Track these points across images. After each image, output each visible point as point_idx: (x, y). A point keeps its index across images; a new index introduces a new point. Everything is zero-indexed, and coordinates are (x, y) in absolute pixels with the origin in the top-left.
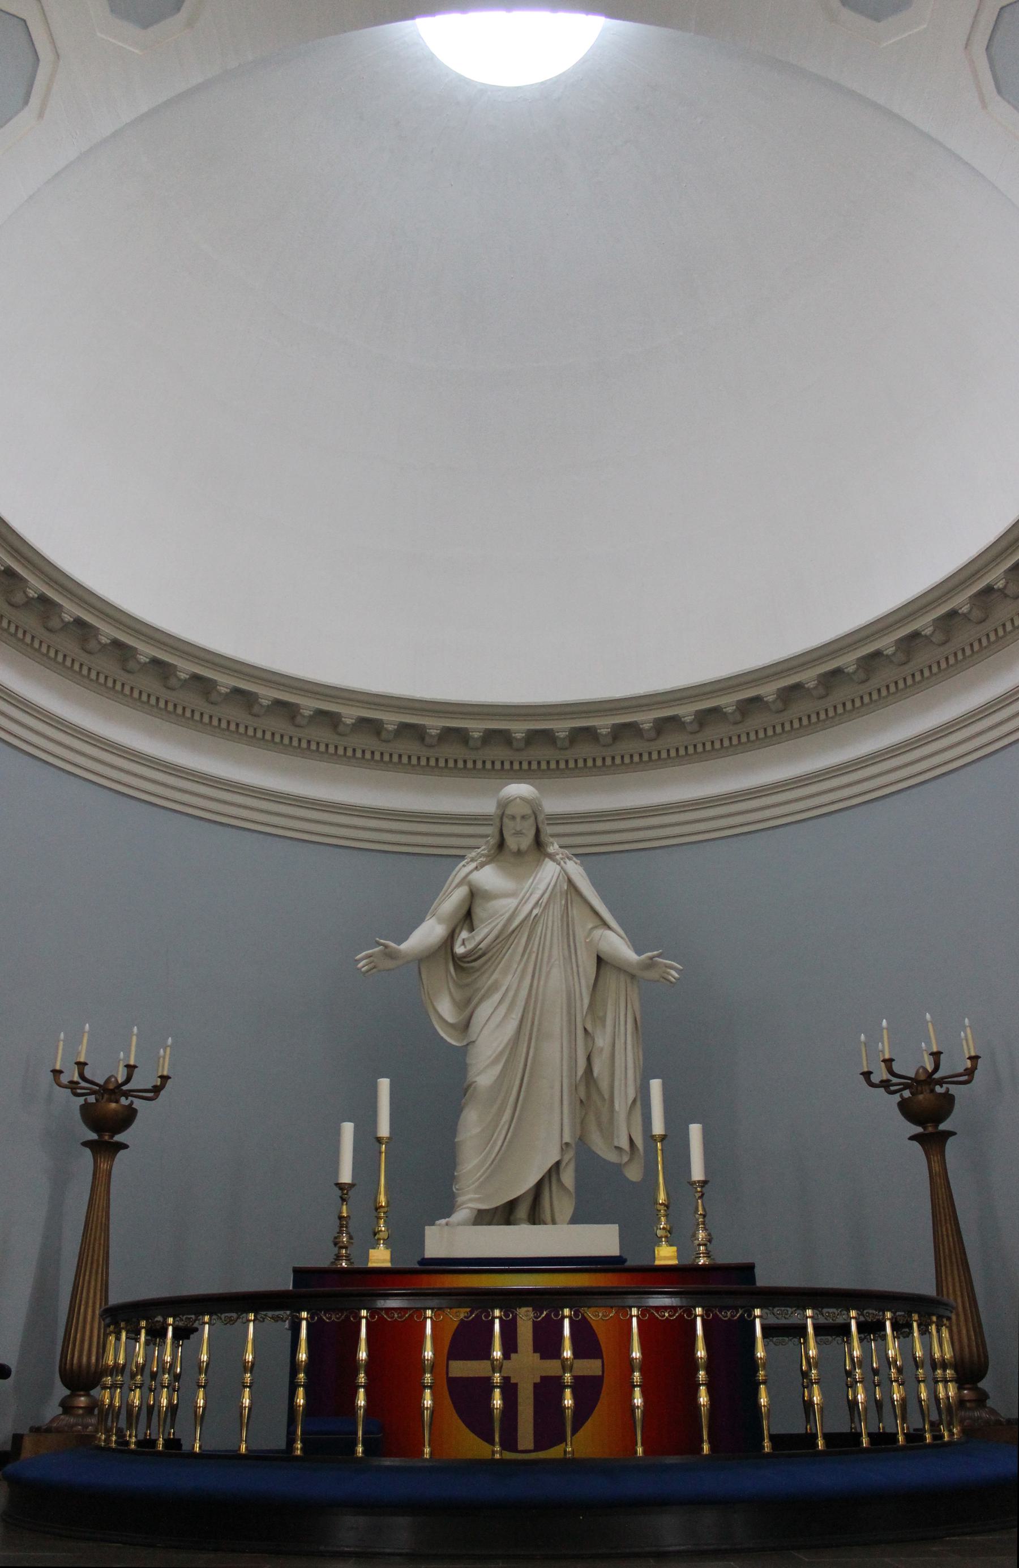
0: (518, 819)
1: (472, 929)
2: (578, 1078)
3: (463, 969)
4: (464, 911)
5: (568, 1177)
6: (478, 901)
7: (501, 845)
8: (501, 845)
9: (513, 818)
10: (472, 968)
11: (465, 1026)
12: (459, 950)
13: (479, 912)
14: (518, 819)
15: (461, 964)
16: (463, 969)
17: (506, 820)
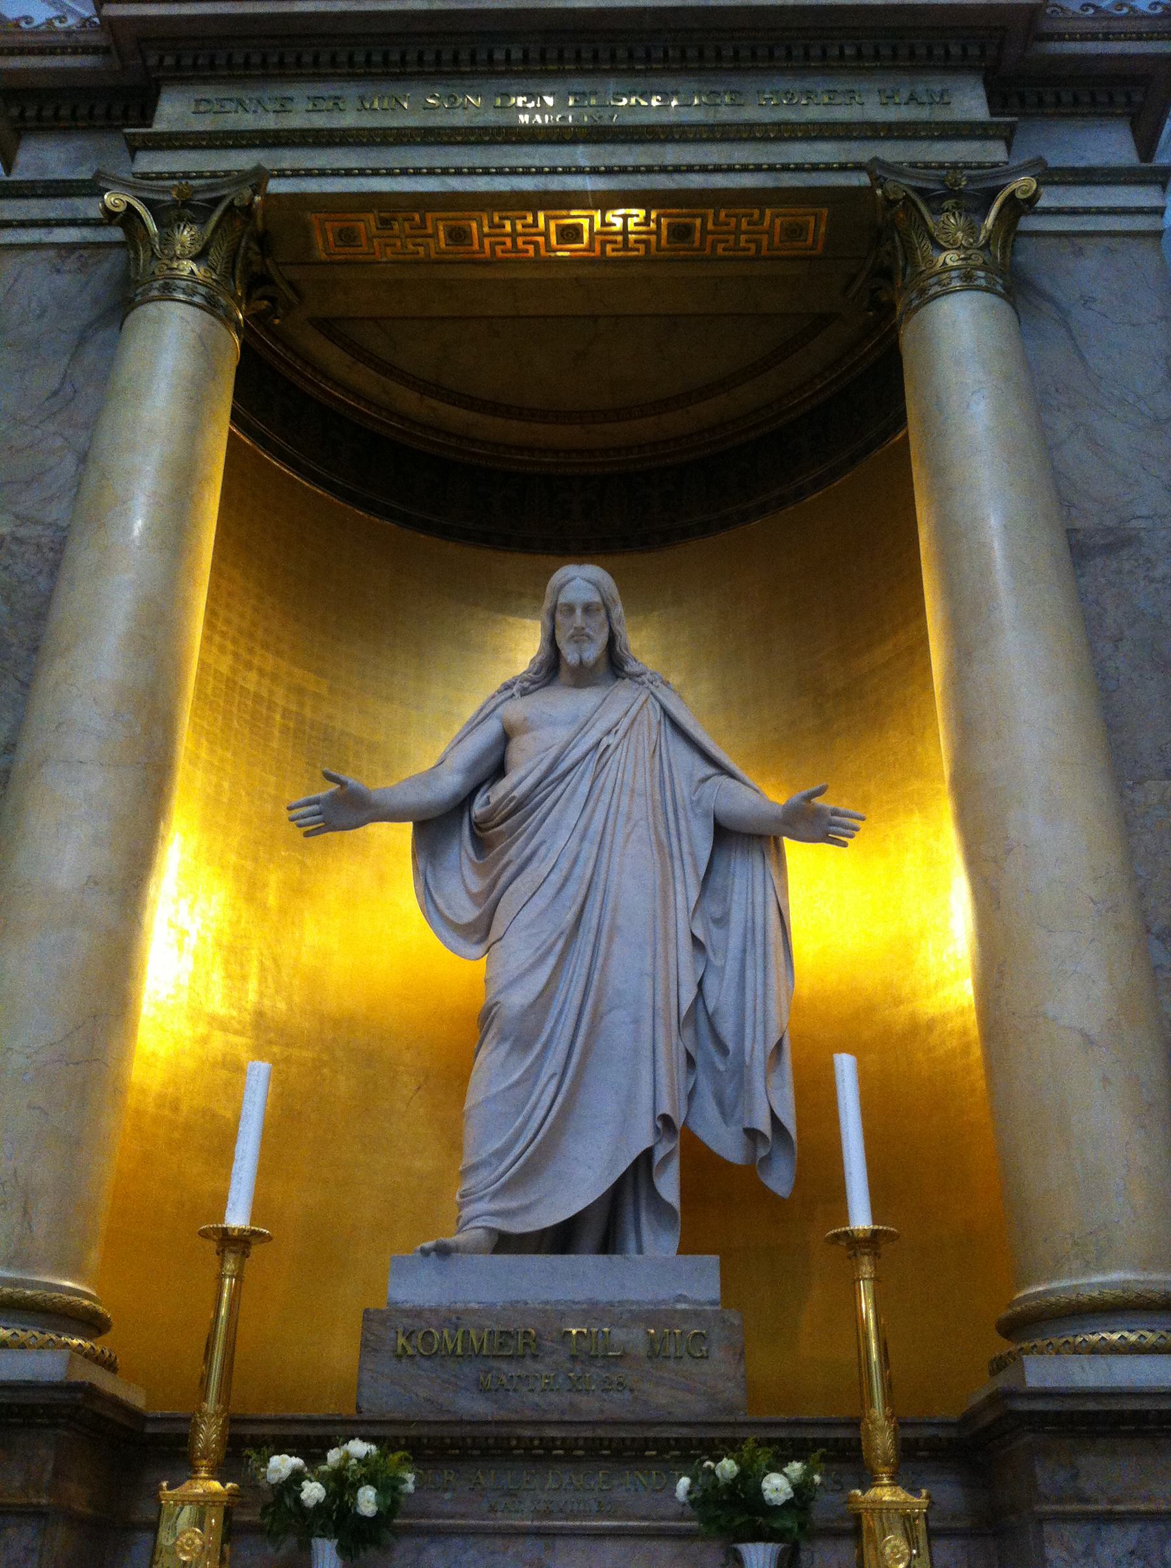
0: (579, 612)
2: (685, 1007)
4: (493, 759)
5: (669, 1186)
9: (570, 609)
10: (501, 833)
14: (579, 612)
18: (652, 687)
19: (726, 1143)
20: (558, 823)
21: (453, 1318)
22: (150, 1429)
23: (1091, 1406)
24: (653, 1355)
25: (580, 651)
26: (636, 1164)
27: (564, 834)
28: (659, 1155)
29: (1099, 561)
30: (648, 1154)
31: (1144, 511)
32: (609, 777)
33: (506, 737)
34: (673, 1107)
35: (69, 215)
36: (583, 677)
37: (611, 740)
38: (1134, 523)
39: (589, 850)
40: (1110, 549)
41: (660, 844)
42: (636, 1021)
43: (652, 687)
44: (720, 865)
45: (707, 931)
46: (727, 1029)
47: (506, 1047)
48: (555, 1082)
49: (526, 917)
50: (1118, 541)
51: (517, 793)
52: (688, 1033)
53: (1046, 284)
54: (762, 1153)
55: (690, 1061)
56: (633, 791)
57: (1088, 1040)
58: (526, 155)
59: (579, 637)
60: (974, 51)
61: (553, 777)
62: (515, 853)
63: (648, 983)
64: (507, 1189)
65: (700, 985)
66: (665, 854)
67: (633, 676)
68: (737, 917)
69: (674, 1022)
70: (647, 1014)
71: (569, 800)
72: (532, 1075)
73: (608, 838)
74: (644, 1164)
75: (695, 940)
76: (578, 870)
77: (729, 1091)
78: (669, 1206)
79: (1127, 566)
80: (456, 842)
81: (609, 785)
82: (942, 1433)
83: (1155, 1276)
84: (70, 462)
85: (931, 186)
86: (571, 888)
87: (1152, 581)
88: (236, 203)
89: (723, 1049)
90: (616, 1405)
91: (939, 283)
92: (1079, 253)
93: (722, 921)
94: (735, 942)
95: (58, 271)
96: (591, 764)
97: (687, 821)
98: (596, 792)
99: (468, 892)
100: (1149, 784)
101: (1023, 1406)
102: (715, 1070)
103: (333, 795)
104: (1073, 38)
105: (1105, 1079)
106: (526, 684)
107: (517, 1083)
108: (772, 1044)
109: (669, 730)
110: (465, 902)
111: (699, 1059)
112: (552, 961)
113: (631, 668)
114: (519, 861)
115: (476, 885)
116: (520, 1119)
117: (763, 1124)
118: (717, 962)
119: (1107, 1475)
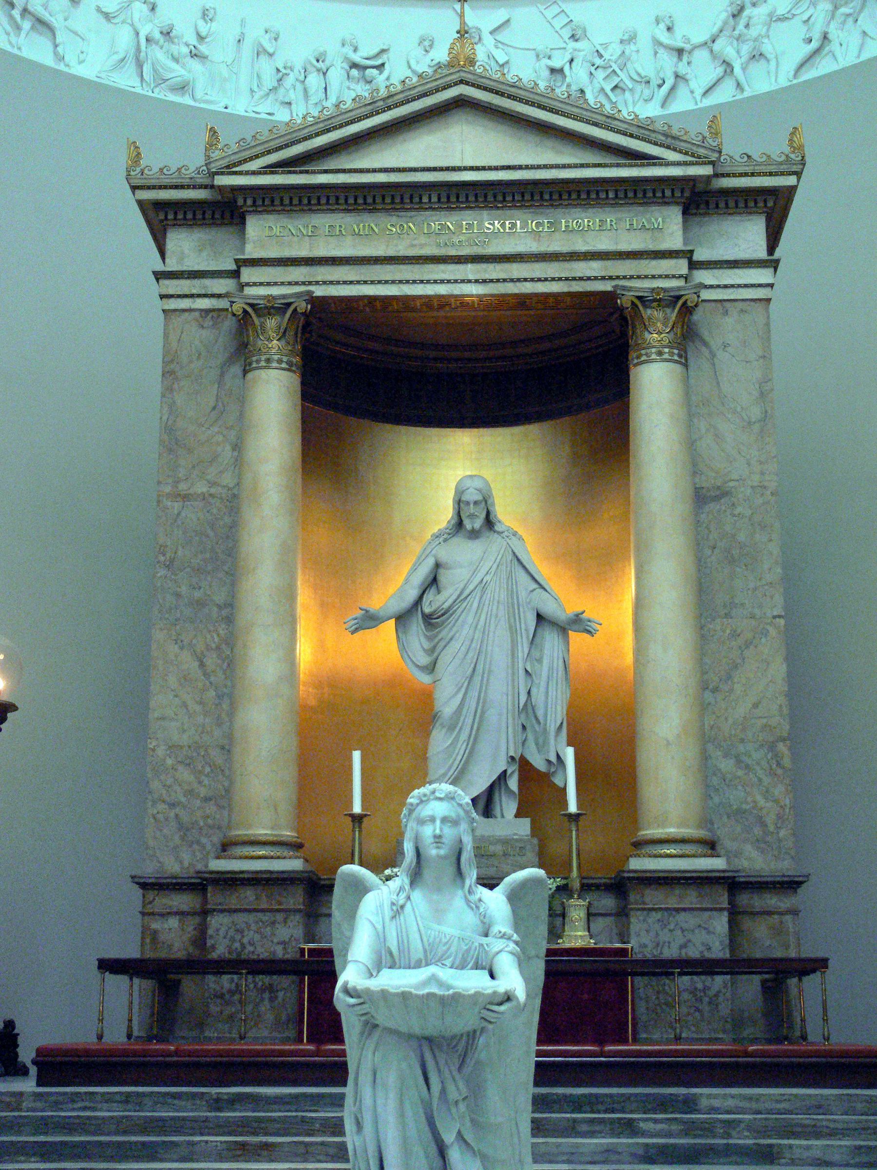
0: (472, 505)
1: (439, 592)
2: (521, 707)
3: (430, 624)
4: (432, 576)
6: (441, 571)
7: (460, 524)
9: (468, 503)
10: (437, 623)
11: (431, 668)
12: (427, 610)
13: (443, 578)
15: (429, 620)
16: (430, 624)
17: (462, 505)
18: (508, 541)
19: (539, 763)
20: (464, 622)
22: (322, 882)
23: (648, 875)
24: (505, 855)
25: (473, 523)
26: (499, 778)
27: (467, 627)
28: (509, 772)
29: (712, 505)
30: (505, 772)
31: (736, 477)
33: (438, 565)
34: (515, 752)
35: (203, 292)
36: (474, 535)
37: (488, 578)
38: (731, 484)
39: (478, 635)
40: (717, 498)
41: (511, 627)
42: (500, 714)
43: (508, 541)
44: (539, 631)
45: (533, 666)
46: (540, 714)
47: (444, 730)
48: (465, 744)
49: (451, 669)
50: (721, 494)
51: (446, 606)
52: (523, 716)
54: (552, 770)
55: (524, 727)
56: (498, 602)
57: (668, 743)
58: (443, 272)
59: (472, 516)
60: (678, 194)
61: (462, 598)
62: (444, 633)
63: (505, 697)
65: (529, 693)
66: (513, 631)
67: (499, 533)
68: (545, 662)
69: (517, 710)
70: (505, 711)
71: (469, 610)
72: (456, 739)
73: (487, 628)
74: (503, 776)
75: (526, 671)
76: (473, 645)
77: (541, 741)
78: (514, 793)
79: (723, 508)
80: (414, 620)
81: (487, 602)
82: (608, 881)
83: (682, 830)
84: (227, 453)
85: (646, 294)
86: (470, 655)
87: (734, 516)
88: (298, 309)
89: (538, 722)
91: (646, 354)
92: (726, 313)
93: (540, 661)
94: (544, 674)
95: (203, 327)
97: (524, 612)
98: (481, 605)
99: (422, 646)
100: (718, 620)
101: (626, 875)
102: (535, 731)
103: (363, 615)
104: (734, 175)
105: (673, 758)
106: (445, 536)
107: (451, 744)
108: (558, 724)
109: (516, 563)
110: (422, 653)
111: (528, 726)
112: (463, 690)
113: (498, 527)
114: (447, 640)
115: (427, 645)
116: (451, 760)
117: (553, 759)
118: (536, 681)
119: (653, 896)
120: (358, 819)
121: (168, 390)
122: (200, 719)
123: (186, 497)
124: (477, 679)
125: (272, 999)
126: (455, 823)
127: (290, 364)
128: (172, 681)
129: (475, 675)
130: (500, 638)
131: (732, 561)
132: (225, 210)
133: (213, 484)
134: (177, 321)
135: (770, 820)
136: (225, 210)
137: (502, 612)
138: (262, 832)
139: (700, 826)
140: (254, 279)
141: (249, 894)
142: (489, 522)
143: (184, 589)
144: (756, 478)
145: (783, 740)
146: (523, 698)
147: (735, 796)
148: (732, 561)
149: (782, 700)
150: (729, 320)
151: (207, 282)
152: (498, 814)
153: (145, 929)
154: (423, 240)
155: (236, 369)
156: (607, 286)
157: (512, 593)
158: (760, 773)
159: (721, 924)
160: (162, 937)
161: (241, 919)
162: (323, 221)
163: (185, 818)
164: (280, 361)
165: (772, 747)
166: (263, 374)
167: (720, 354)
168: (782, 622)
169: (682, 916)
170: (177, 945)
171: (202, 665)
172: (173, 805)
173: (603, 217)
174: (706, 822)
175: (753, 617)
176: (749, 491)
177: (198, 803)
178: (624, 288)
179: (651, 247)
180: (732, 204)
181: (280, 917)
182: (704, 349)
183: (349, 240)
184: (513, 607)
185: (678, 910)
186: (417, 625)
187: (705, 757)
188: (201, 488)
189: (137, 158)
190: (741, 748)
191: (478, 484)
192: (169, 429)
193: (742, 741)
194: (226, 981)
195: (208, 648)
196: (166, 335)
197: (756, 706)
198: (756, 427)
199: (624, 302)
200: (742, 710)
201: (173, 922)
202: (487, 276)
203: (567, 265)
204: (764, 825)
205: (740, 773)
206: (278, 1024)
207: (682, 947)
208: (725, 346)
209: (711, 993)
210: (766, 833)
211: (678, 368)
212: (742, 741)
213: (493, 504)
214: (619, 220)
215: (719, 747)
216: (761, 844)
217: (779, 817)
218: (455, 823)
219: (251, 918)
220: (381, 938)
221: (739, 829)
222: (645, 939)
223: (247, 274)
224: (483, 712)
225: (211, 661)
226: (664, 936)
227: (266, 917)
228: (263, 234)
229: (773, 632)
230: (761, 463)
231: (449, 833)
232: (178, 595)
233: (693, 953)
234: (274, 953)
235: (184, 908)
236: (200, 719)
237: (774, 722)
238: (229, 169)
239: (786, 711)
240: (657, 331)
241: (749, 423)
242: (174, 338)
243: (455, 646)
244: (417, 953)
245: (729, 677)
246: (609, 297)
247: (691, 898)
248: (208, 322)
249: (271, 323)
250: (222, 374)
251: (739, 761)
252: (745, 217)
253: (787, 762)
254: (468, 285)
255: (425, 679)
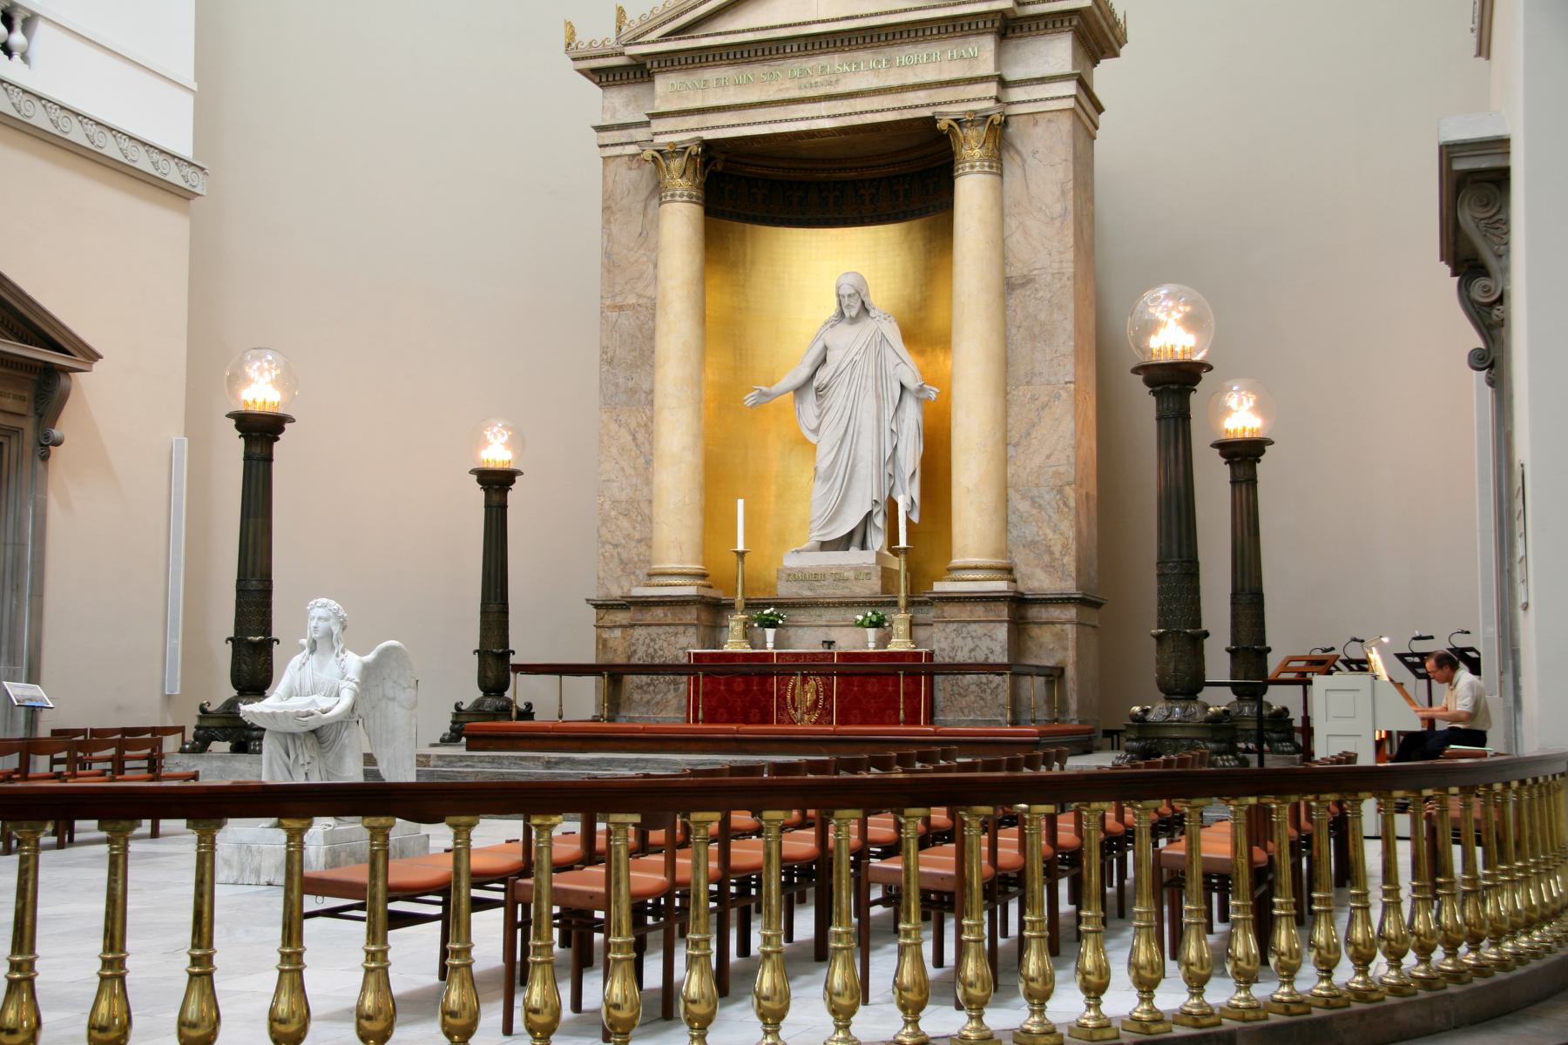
7: (842, 314)
8: (842, 314)
11: (816, 431)
21: (801, 570)
30: (870, 513)
32: (857, 372)
33: (826, 348)
36: (854, 320)
40: (1023, 285)
41: (878, 396)
50: (1027, 281)
53: (1019, 147)
60: (989, 25)
61: (837, 374)
64: (824, 526)
74: (869, 515)
90: (846, 592)
92: (1036, 124)
96: (849, 370)
120: (741, 555)
121: (607, 222)
122: (634, 480)
123: (621, 308)
124: (849, 438)
125: (676, 690)
126: (327, 620)
127: (690, 196)
128: (614, 450)
129: (847, 434)
130: (868, 406)
131: (1034, 338)
132: (639, 71)
133: (640, 296)
134: (612, 165)
135: (1057, 549)
136: (639, 71)
137: (870, 383)
138: (670, 565)
139: (995, 556)
140: (661, 129)
141: (659, 612)
142: (865, 309)
143: (621, 380)
144: (1056, 265)
145: (1069, 484)
146: (889, 452)
147: (1030, 531)
148: (1034, 338)
149: (1070, 452)
150: (1039, 130)
151: (632, 131)
152: (869, 544)
153: (598, 638)
154: (788, 84)
155: (655, 202)
156: (927, 113)
157: (880, 367)
158: (1051, 512)
159: (1002, 632)
160: (611, 644)
161: (654, 630)
162: (710, 74)
163: (624, 556)
164: (681, 196)
165: (1060, 491)
166: (667, 207)
167: (1030, 161)
168: (1072, 386)
169: (973, 627)
170: (620, 649)
171: (634, 439)
172: (616, 546)
173: (929, 51)
174: (1005, 551)
175: (1049, 383)
176: (1049, 278)
177: (633, 544)
178: (942, 113)
179: (968, 75)
180: (1042, 26)
181: (681, 629)
182: (1017, 158)
183: (732, 90)
184: (880, 378)
185: (969, 622)
186: (810, 397)
187: (1004, 500)
188: (632, 300)
189: (572, 34)
190: (1035, 492)
191: (851, 279)
192: (607, 254)
193: (1037, 485)
194: (645, 679)
195: (639, 425)
196: (604, 177)
197: (1048, 457)
198: (1057, 223)
199: (942, 125)
200: (1038, 460)
201: (618, 633)
202: (837, 112)
203: (899, 96)
204: (1052, 553)
205: (1034, 512)
206: (679, 708)
207: (971, 651)
208: (1035, 153)
209: (993, 685)
210: (1053, 560)
211: (988, 177)
212: (1037, 485)
213: (868, 294)
214: (942, 52)
215: (1017, 491)
216: (1050, 568)
217: (1065, 546)
218: (327, 620)
219: (661, 630)
220: (292, 678)
221: (1032, 556)
222: (944, 644)
223: (658, 125)
224: (854, 466)
225: (641, 436)
226: (959, 642)
227: (671, 629)
228: (668, 90)
229: (1064, 394)
230: (1061, 253)
231: (322, 625)
232: (617, 385)
233: (980, 657)
234: (677, 657)
235: (625, 622)
236: (634, 480)
237: (1062, 469)
238: (634, 41)
239: (1072, 460)
240: (972, 149)
241: (1052, 219)
242: (610, 180)
243: (832, 413)
244: (308, 687)
245: (1029, 434)
246: (931, 121)
247: (979, 611)
248: (635, 165)
249: (676, 164)
250: (645, 208)
251: (1033, 502)
252: (1055, 36)
253: (1072, 503)
254: (821, 118)
255: (812, 438)
